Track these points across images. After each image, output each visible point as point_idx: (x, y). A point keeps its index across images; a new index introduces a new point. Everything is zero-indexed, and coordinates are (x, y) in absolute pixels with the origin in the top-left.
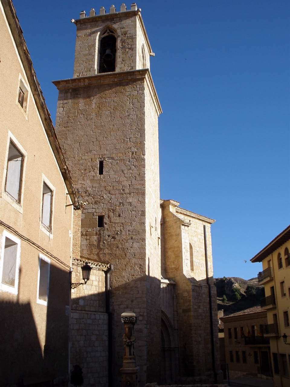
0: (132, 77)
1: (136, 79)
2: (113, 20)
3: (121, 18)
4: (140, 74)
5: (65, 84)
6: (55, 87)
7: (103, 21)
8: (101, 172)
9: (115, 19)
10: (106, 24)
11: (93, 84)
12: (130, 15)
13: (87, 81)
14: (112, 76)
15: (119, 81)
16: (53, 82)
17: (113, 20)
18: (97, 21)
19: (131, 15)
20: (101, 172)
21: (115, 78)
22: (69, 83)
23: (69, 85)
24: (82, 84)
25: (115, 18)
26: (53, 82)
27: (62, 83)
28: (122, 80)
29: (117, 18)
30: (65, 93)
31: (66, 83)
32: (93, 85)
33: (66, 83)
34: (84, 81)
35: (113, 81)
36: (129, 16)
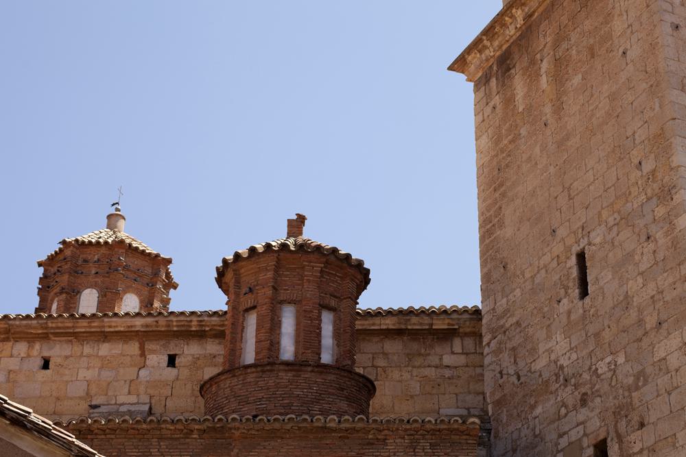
5: (478, 55)
6: (461, 77)
8: (584, 293)
11: (534, 12)
13: (519, 14)
16: (451, 68)
20: (584, 293)
22: (485, 47)
23: (487, 52)
24: (511, 31)
26: (451, 68)
27: (470, 58)
31: (480, 52)
32: (536, 14)
33: (480, 52)
34: (512, 17)
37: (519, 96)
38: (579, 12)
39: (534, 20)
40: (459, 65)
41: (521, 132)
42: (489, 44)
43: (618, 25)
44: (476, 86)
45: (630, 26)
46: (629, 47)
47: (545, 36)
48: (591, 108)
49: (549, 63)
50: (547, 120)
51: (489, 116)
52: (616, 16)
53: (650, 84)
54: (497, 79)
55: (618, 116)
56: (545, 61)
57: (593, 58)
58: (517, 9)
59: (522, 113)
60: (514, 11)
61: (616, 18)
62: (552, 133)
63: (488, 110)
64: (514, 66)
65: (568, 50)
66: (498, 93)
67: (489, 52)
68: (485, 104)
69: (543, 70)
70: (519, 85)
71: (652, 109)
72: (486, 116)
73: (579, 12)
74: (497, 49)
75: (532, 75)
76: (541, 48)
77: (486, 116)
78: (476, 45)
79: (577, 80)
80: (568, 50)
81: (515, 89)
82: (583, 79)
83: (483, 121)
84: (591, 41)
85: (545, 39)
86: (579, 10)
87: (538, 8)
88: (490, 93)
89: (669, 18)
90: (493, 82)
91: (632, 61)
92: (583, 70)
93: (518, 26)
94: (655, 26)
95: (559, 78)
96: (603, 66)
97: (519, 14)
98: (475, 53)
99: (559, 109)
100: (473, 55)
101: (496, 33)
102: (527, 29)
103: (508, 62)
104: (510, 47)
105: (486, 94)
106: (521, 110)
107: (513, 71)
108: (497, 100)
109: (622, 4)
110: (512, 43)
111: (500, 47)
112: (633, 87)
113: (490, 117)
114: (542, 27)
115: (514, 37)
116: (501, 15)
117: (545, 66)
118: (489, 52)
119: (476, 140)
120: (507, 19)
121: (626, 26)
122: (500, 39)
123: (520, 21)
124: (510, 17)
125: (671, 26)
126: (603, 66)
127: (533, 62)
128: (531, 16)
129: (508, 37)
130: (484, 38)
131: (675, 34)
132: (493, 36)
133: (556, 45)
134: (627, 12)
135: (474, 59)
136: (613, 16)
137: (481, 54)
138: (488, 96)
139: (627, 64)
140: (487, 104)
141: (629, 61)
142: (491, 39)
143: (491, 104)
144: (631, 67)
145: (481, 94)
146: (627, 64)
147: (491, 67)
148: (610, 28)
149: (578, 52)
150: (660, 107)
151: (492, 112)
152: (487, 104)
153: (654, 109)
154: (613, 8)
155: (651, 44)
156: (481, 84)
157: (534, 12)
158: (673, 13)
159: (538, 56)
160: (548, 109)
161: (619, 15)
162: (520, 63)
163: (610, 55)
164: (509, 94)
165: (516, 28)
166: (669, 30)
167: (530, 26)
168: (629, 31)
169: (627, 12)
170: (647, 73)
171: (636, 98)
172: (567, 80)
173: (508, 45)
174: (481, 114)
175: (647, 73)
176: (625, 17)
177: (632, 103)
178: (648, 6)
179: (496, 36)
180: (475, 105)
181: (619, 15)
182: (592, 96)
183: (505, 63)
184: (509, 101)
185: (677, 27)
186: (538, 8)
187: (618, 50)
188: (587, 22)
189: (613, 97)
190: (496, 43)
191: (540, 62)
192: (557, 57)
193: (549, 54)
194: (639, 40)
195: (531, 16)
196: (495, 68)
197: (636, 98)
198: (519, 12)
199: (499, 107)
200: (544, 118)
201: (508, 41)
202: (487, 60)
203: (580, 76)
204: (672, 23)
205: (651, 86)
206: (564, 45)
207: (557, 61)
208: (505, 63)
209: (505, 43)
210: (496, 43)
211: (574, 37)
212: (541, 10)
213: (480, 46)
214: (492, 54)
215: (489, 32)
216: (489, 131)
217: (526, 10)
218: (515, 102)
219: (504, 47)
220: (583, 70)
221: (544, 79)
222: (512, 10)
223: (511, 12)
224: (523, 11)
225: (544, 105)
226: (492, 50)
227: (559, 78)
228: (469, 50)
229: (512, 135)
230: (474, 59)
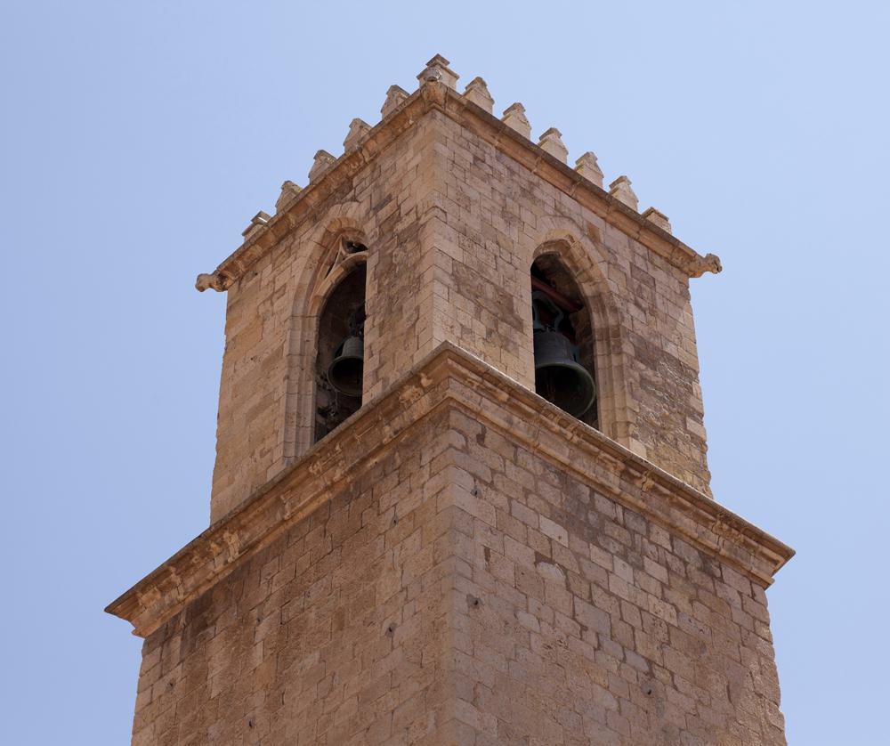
0: (398, 423)
1: (414, 423)
2: (351, 188)
3: (378, 160)
4: (425, 390)
5: (158, 596)
7: (315, 219)
9: (355, 181)
10: (325, 224)
11: (258, 542)
12: (406, 126)
13: (234, 541)
14: (319, 465)
15: (351, 471)
16: (110, 610)
17: (351, 188)
18: (291, 232)
19: (411, 122)
21: (335, 464)
22: (172, 585)
23: (174, 593)
24: (217, 566)
25: (356, 174)
26: (110, 610)
27: (144, 598)
28: (364, 460)
29: (362, 169)
30: (162, 645)
31: (163, 591)
32: (261, 547)
33: (163, 591)
34: (222, 544)
35: (328, 488)
36: (404, 130)
37: (215, 672)
38: (329, 554)
39: (256, 555)
40: (125, 606)
41: (211, 730)
42: (178, 580)
43: (386, 585)
44: (147, 644)
45: (404, 589)
46: (398, 622)
47: (269, 582)
48: (328, 709)
49: (271, 625)
50: (254, 718)
51: (160, 696)
52: (385, 569)
53: (424, 685)
54: (182, 639)
55: (368, 729)
56: (265, 622)
57: (341, 630)
58: (232, 533)
59: (216, 700)
60: (226, 535)
61: (384, 573)
62: (260, 741)
63: (161, 687)
64: (214, 623)
65: (303, 610)
66: (182, 661)
67: (177, 594)
68: (157, 677)
69: (259, 637)
70: (218, 652)
71: (423, 726)
72: (156, 695)
73: (329, 554)
74: (190, 590)
75: (241, 640)
76: (260, 600)
77: (156, 695)
78: (157, 580)
79: (311, 660)
80: (303, 610)
81: (209, 660)
82: (322, 660)
83: (151, 703)
84: (342, 603)
85: (268, 587)
86: (329, 550)
87: (265, 536)
88: (169, 659)
89: (467, 588)
90: (177, 642)
91: (401, 645)
92: (322, 646)
93: (230, 560)
94: (442, 595)
95: (282, 652)
96: (355, 645)
97: (234, 541)
98: (154, 592)
99: (276, 702)
100: (150, 594)
101: (193, 565)
102: (243, 566)
103: (205, 614)
104: (211, 590)
105: (161, 660)
106: (213, 695)
107: (210, 630)
108: (177, 673)
109: (397, 553)
110: (216, 585)
111: (196, 588)
112: (399, 686)
113: (163, 698)
114: (267, 568)
115: (221, 577)
116: (205, 538)
117: (263, 630)
118: (177, 594)
119: (134, 733)
120: (213, 545)
121: (399, 588)
122: (197, 575)
123: (234, 553)
124: (219, 545)
125: (467, 601)
126: (355, 645)
127: (244, 621)
128: (252, 547)
129: (211, 575)
130: (172, 569)
131: (472, 613)
132: (188, 569)
133: (286, 599)
134: (402, 566)
135: (151, 601)
136: (381, 570)
137: (163, 595)
138: (164, 665)
139: (393, 648)
140: (161, 676)
141: (396, 645)
142: (183, 574)
143: (168, 678)
144: (398, 654)
145: (154, 658)
146: (393, 648)
147: (176, 618)
148: (374, 586)
149: (319, 616)
150: (436, 725)
151: (167, 692)
152: (161, 676)
153: (426, 727)
154: (383, 557)
155: (433, 622)
156: (156, 642)
157: (258, 542)
158: (472, 581)
159: (255, 613)
160: (258, 700)
161: (390, 569)
162: (225, 620)
163: (369, 629)
164: (199, 665)
165: (226, 562)
166: (464, 606)
167: (248, 563)
168: (401, 598)
169: (402, 566)
170: (422, 667)
171: (401, 705)
172: (294, 659)
173: (210, 586)
174: (149, 691)
175: (422, 667)
176: (399, 574)
177: (393, 712)
178: (435, 563)
179: (192, 570)
180: (141, 676)
181: (390, 569)
182: (331, 690)
183: (199, 615)
184: (197, 678)
185: (476, 603)
186: (265, 536)
187: (381, 623)
188: (338, 572)
189: (365, 697)
190: (190, 582)
191: (256, 621)
192: (285, 619)
193: (272, 613)
194: (415, 613)
195: (252, 547)
196: (182, 620)
197: (401, 705)
198: (235, 538)
199: (180, 684)
200: (250, 715)
201: (210, 581)
202: (172, 606)
203: (317, 655)
204: (469, 596)
205: (427, 689)
206: (298, 603)
207: (284, 625)
208: (199, 615)
209: (204, 584)
210: (190, 582)
211: (316, 591)
212: (269, 541)
213: (164, 581)
214: (181, 597)
215: (182, 561)
216: (157, 721)
217: (247, 537)
218: (206, 679)
219: (202, 590)
220: (322, 646)
221: (258, 651)
222: (224, 533)
223: (221, 536)
224: (240, 537)
225: (253, 693)
226: (181, 590)
227: (282, 652)
228: (145, 585)
229: (195, 734)
230: (151, 601)
